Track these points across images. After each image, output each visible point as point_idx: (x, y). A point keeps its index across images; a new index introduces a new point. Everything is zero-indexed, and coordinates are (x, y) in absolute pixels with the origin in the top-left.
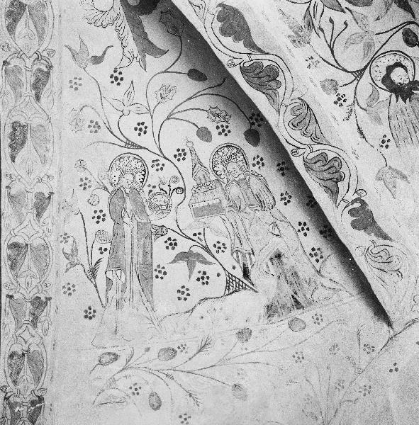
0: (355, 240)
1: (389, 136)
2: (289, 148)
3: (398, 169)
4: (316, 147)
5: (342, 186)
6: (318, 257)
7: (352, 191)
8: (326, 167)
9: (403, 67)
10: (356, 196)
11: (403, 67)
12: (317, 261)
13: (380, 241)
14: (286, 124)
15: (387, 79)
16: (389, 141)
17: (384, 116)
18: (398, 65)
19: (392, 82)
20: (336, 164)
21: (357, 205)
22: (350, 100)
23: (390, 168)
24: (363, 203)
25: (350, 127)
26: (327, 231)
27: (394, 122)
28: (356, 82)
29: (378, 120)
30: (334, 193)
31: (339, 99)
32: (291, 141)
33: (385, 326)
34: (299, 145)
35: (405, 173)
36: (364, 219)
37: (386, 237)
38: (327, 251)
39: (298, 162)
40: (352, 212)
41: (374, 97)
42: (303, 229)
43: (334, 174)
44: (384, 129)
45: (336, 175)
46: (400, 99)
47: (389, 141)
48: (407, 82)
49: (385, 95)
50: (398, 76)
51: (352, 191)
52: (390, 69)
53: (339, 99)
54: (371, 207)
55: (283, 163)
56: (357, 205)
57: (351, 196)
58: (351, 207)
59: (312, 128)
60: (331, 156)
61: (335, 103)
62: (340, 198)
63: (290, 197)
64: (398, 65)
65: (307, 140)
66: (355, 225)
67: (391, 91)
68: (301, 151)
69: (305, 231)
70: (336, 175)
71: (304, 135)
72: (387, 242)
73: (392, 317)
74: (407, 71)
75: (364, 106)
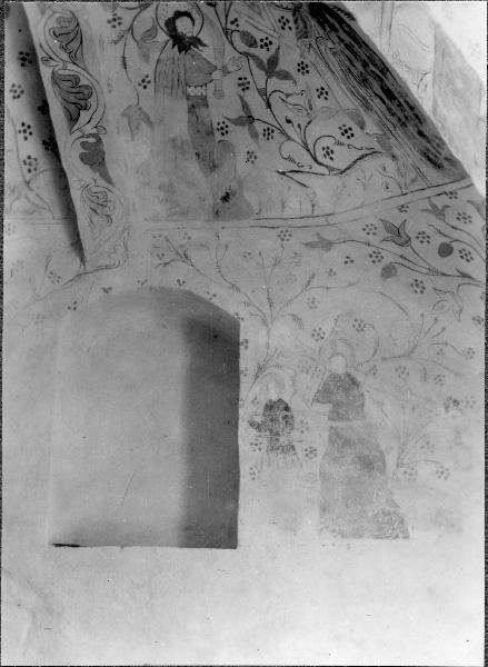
0: (79, 174)
1: (151, 78)
2: (40, 54)
3: (148, 112)
4: (71, 66)
5: (84, 116)
6: (32, 168)
7: (93, 123)
8: (74, 90)
9: (192, 19)
10: (95, 131)
11: (192, 19)
12: (30, 171)
13: (102, 182)
14: (47, 29)
15: (171, 23)
16: (149, 82)
17: (154, 56)
18: (187, 14)
19: (175, 29)
20: (86, 92)
21: (92, 140)
22: (126, 25)
23: (140, 109)
24: (99, 140)
25: (116, 51)
26: (50, 145)
27: (160, 67)
28: (136, 12)
29: (146, 58)
30: (73, 119)
31: (115, 20)
32: (45, 46)
33: (78, 261)
34: (53, 56)
35: (152, 118)
36: (94, 156)
37: (110, 181)
38: (43, 163)
39: (46, 72)
40: (83, 144)
41: (151, 33)
42: (25, 131)
43: (79, 99)
44: (148, 69)
45: (82, 103)
46: (176, 47)
47: (149, 82)
48: (189, 35)
49: (162, 37)
50: (183, 26)
51: (93, 123)
52: (179, 14)
53: (115, 20)
54: (106, 148)
55: (27, 54)
56: (92, 140)
57: (89, 129)
58: (85, 140)
59: (74, 45)
60: (83, 82)
61: (109, 22)
62: (76, 127)
63: (22, 92)
64: (187, 14)
65: (65, 56)
66: (83, 158)
67: (172, 36)
68: (53, 63)
69: (27, 134)
70: (82, 103)
71: (64, 48)
72: (110, 187)
73: (87, 257)
74: (193, 24)
75: (138, 38)
